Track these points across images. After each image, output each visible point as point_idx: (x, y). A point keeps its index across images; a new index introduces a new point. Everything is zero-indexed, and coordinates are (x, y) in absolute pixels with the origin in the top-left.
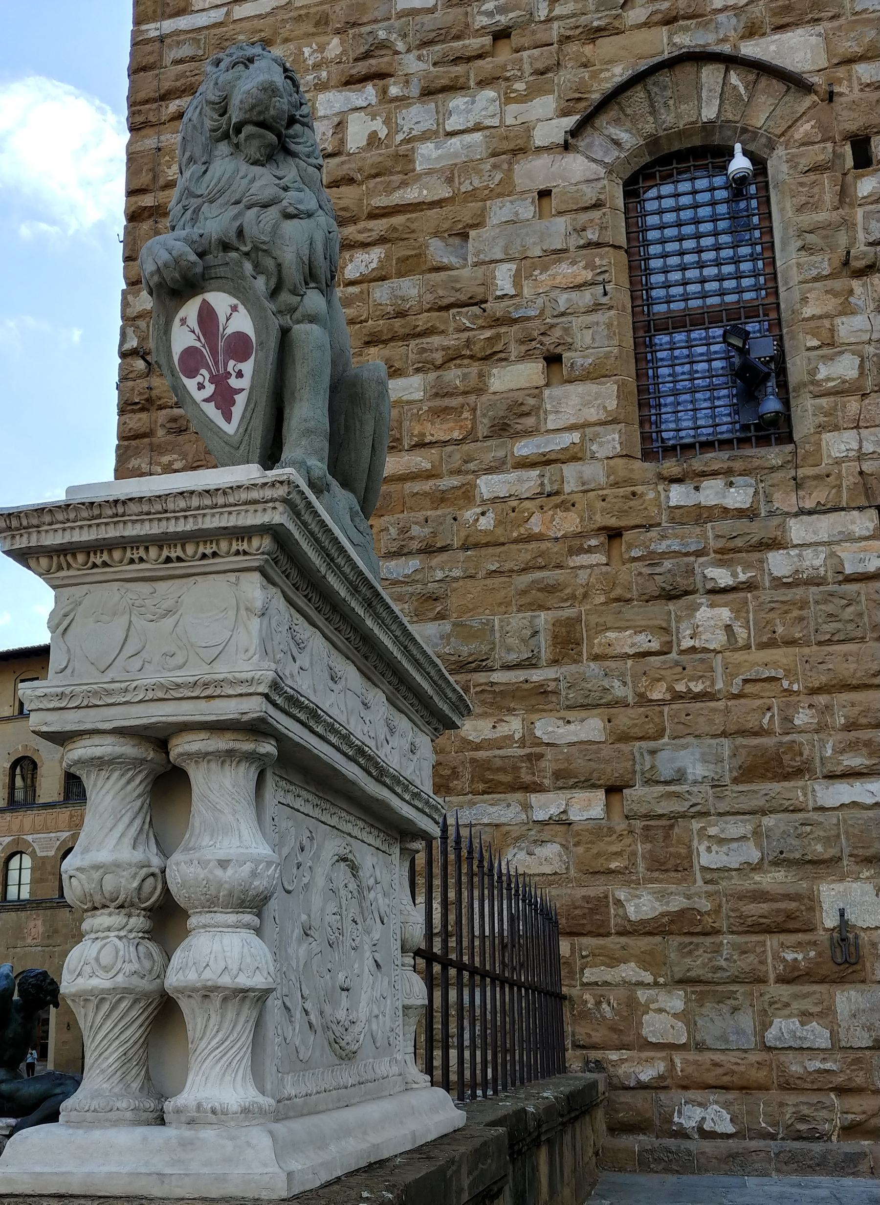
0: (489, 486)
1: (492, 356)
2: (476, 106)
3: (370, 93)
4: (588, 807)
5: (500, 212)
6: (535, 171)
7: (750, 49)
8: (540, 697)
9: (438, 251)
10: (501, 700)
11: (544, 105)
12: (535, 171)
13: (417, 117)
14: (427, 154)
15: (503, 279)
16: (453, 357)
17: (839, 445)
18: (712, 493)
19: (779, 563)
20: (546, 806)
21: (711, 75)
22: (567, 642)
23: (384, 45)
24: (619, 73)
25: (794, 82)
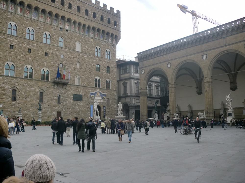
0: (7, 101)
1: (7, 96)
2: (7, 86)
3: (3, 84)
4: (9, 112)
5: (8, 91)
6: (9, 89)
7: (17, 87)
8: (8, 108)
9: (6, 92)
10: (7, 108)
11: (10, 87)
12: (9, 89)
13: (5, 86)
14: (5, 87)
15: (8, 93)
16: (6, 96)
17: (17, 101)
18: (14, 102)
19: (15, 105)
20: (8, 112)
21: (15, 87)
22: (9, 107)
23: (4, 82)
24: (12, 86)
25: (18, 88)
